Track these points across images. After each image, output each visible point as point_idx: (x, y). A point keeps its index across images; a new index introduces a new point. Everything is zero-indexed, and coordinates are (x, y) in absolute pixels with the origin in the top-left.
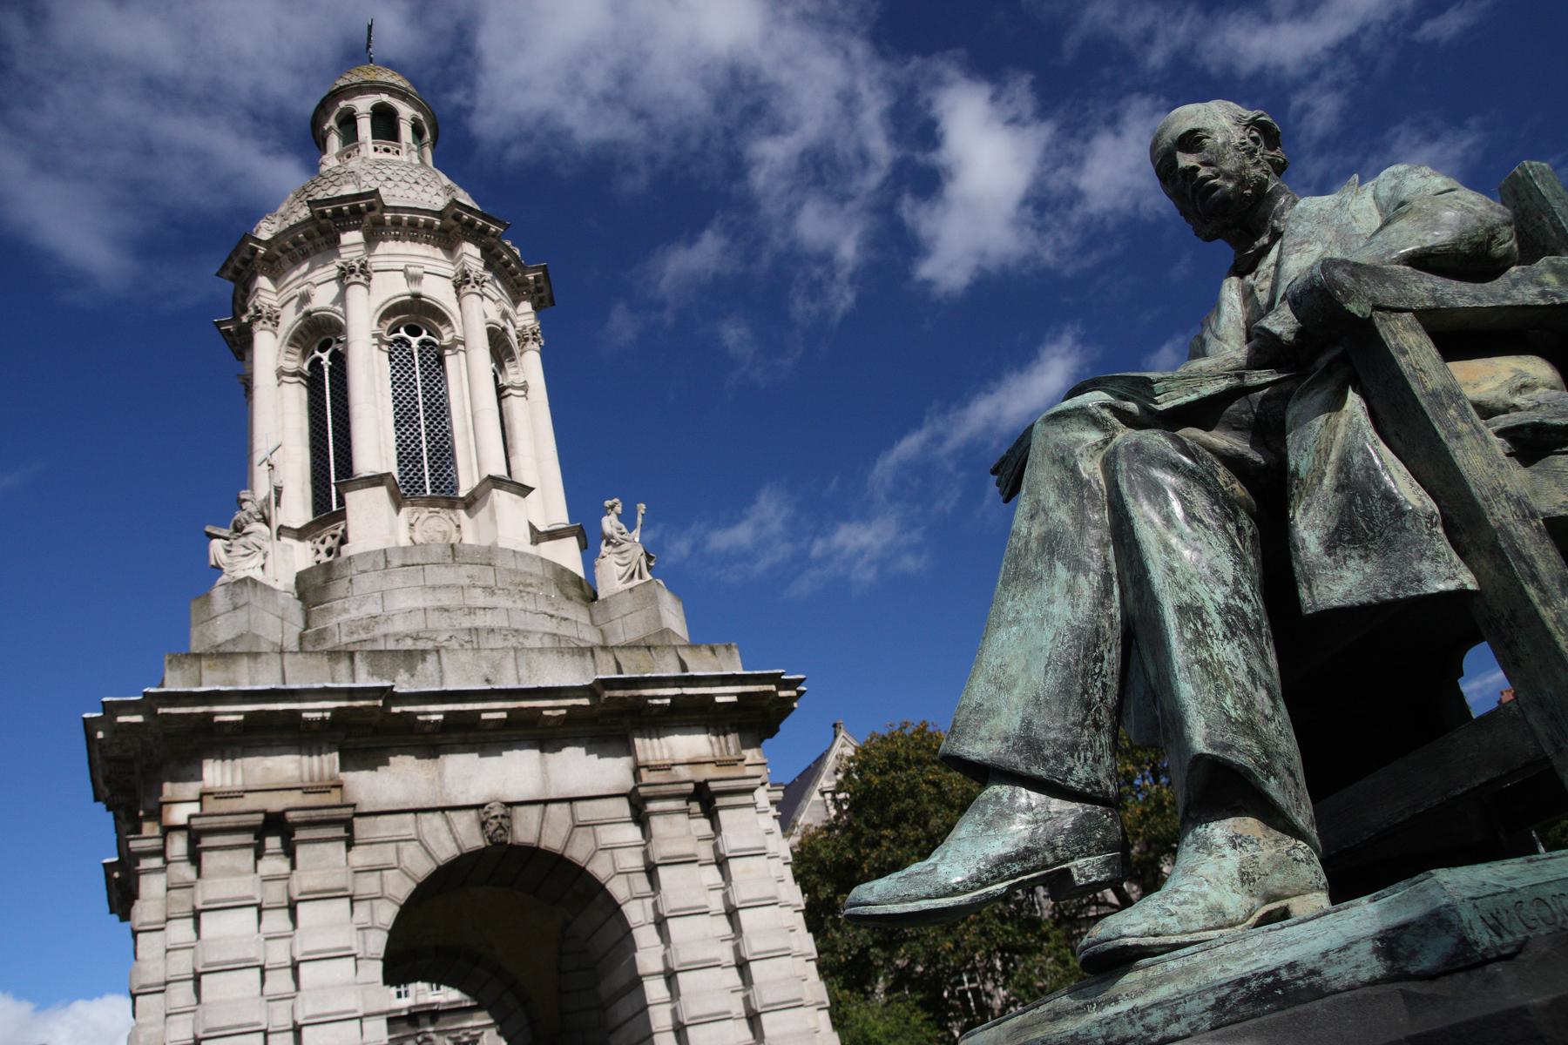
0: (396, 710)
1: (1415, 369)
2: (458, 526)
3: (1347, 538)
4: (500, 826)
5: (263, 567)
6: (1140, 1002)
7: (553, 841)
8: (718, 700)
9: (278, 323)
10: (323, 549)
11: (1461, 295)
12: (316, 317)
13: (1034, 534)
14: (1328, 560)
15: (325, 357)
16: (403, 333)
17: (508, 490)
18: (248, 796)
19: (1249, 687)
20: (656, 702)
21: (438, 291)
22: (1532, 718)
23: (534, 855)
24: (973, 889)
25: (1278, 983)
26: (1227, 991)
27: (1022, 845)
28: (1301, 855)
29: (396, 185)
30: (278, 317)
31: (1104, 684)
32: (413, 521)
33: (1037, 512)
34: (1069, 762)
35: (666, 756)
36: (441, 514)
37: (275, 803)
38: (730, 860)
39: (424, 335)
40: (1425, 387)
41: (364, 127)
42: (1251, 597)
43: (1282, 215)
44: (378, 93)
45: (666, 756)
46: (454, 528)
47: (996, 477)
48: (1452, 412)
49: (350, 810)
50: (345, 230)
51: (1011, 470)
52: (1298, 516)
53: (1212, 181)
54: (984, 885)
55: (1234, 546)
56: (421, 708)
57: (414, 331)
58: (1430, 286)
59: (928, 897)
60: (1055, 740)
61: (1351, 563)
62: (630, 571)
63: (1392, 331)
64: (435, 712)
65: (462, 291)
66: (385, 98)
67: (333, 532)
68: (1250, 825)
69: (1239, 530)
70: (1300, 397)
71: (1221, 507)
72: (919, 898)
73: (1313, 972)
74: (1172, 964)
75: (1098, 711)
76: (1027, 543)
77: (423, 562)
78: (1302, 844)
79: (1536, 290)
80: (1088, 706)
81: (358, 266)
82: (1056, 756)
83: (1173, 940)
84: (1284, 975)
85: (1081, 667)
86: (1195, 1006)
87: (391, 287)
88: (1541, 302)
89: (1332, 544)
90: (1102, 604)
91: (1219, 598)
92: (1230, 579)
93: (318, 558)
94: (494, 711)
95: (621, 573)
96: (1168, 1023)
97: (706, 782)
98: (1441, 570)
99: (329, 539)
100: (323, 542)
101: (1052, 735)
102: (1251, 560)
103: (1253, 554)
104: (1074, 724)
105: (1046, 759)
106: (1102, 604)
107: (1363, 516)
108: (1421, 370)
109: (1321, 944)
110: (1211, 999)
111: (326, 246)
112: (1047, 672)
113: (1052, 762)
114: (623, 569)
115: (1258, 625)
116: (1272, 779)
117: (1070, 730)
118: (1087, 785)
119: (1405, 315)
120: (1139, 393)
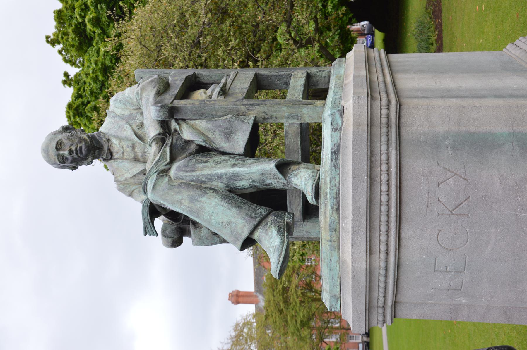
3: (228, 136)
6: (329, 186)
13: (187, 204)
14: (232, 143)
24: (284, 238)
25: (335, 153)
26: (333, 164)
33: (181, 202)
34: (258, 212)
47: (148, 235)
48: (207, 103)
51: (150, 227)
52: (215, 146)
53: (78, 147)
59: (282, 248)
60: (251, 213)
61: (235, 138)
69: (214, 155)
70: (182, 133)
72: (282, 250)
73: (335, 145)
74: (322, 180)
76: (189, 207)
79: (179, 81)
82: (256, 214)
83: (317, 178)
84: (333, 151)
86: (333, 172)
88: (183, 81)
92: (229, 158)
96: (335, 180)
105: (255, 217)
106: (218, 192)
107: (225, 129)
109: (329, 142)
110: (333, 168)
112: (231, 210)
113: (257, 215)
117: (250, 209)
118: (266, 211)
120: (160, 165)
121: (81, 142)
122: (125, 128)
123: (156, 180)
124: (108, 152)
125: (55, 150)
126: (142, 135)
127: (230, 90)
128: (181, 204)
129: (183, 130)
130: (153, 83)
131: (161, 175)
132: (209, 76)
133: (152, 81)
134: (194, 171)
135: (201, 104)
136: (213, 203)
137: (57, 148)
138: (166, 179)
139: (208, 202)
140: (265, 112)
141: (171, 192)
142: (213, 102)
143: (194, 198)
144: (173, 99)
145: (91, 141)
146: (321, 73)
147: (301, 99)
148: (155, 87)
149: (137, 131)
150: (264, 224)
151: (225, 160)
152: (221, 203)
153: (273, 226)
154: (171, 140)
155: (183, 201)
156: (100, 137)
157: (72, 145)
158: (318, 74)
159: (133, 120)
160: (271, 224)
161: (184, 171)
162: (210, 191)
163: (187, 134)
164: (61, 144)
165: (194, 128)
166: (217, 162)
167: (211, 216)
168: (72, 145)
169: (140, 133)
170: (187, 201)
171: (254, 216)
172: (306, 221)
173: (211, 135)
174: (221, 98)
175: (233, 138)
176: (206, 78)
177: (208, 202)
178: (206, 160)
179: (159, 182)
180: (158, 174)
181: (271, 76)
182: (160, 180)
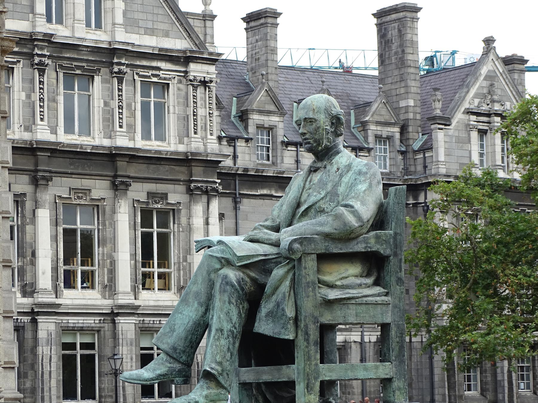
1: (306, 274)
13: (193, 290)
14: (264, 319)
19: (227, 352)
22: (296, 371)
24: (151, 381)
27: (165, 372)
28: (223, 393)
31: (197, 337)
40: (306, 280)
42: (237, 328)
43: (331, 157)
48: (310, 289)
52: (263, 303)
53: (309, 140)
54: (153, 380)
55: (240, 312)
58: (326, 244)
59: (140, 380)
63: (305, 261)
68: (213, 385)
69: (243, 307)
71: (240, 301)
72: (138, 380)
75: (193, 344)
76: (190, 291)
78: (224, 390)
79: (364, 245)
80: (191, 342)
82: (179, 353)
85: (192, 332)
88: (363, 250)
89: (267, 315)
90: (203, 317)
91: (229, 327)
92: (234, 323)
98: (286, 333)
101: (180, 348)
102: (243, 316)
103: (245, 314)
104: (186, 346)
105: (177, 353)
107: (276, 311)
108: (308, 275)
112: (183, 331)
113: (178, 354)
115: (236, 335)
116: (221, 376)
117: (184, 347)
118: (185, 361)
119: (313, 255)
121: (315, 141)
122: (322, 192)
123: (217, 257)
124: (316, 167)
125: (304, 118)
126: (310, 214)
127: (341, 306)
128: (195, 284)
129: (280, 269)
130: (342, 227)
131: (223, 261)
132: (389, 271)
133: (345, 224)
134: (220, 292)
135: (308, 283)
136: (191, 314)
137: (306, 119)
138: (218, 266)
139: (193, 309)
140: (300, 347)
141: (205, 273)
142: (311, 294)
143: (198, 296)
144: (319, 252)
145: (322, 150)
146: (392, 393)
147: (321, 379)
148: (336, 229)
149: (314, 207)
150: (172, 360)
151: (231, 319)
152: (191, 321)
153: (167, 369)
154: (274, 257)
155: (196, 285)
156: (331, 156)
157: (311, 133)
158: (392, 390)
159: (330, 199)
160: (169, 367)
161: (221, 283)
162: (203, 309)
163: (278, 272)
164: (311, 122)
165: (281, 281)
166: (229, 312)
167: (181, 313)
168: (311, 133)
169: (312, 210)
170: (196, 289)
171: (178, 351)
172: (240, 386)
173: (274, 297)
175: (268, 320)
176: (387, 268)
177: (193, 309)
178: (233, 301)
179: (215, 260)
180: (223, 258)
181: (389, 339)
182: (217, 261)
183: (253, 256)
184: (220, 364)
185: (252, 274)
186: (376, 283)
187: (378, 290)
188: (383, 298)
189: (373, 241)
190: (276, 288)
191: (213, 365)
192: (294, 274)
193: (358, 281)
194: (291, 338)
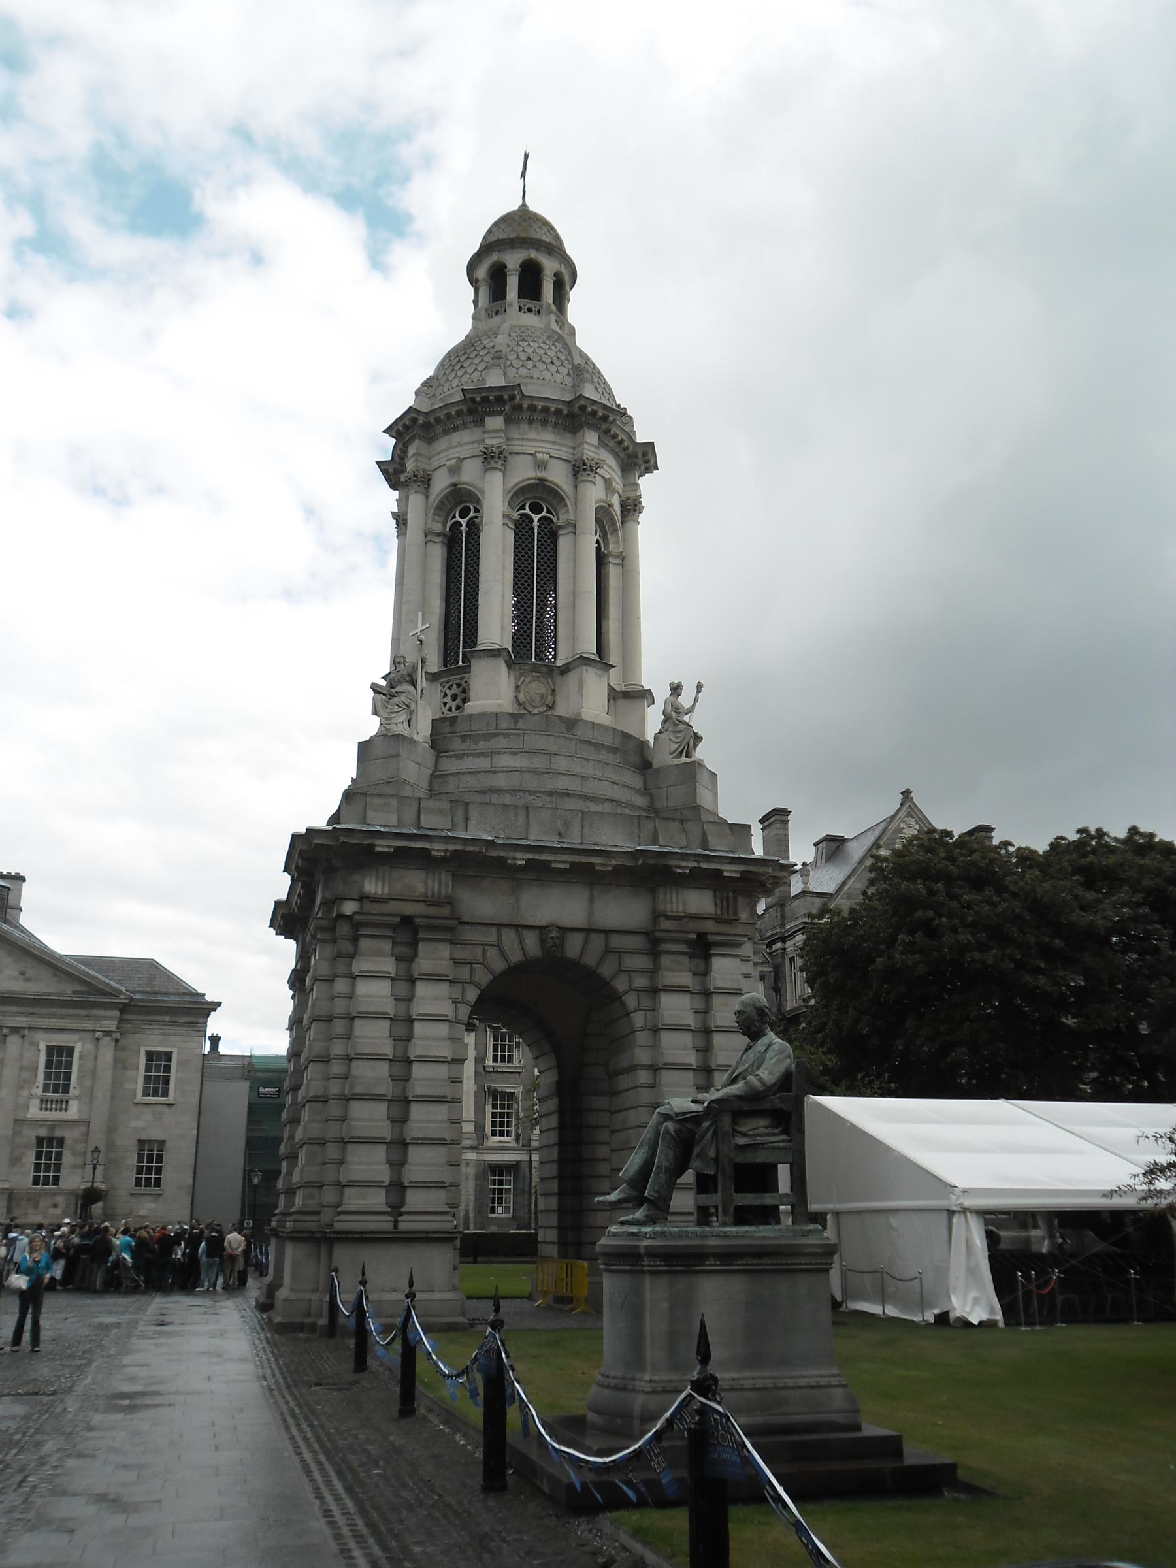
0: (493, 854)
2: (554, 690)
4: (555, 945)
5: (409, 721)
7: (590, 960)
8: (726, 874)
9: (429, 485)
10: (450, 694)
11: (746, 1107)
12: (460, 489)
15: (464, 522)
16: (528, 511)
17: (594, 667)
18: (391, 902)
20: (679, 870)
21: (558, 475)
23: (574, 965)
29: (535, 366)
30: (429, 480)
32: (519, 683)
35: (681, 909)
36: (542, 679)
37: (409, 909)
38: (713, 995)
39: (544, 513)
41: (513, 283)
44: (528, 249)
45: (681, 909)
46: (550, 691)
49: (456, 922)
50: (490, 414)
56: (511, 854)
57: (536, 509)
62: (680, 749)
64: (521, 858)
65: (580, 478)
66: (533, 254)
67: (458, 681)
77: (524, 728)
81: (497, 452)
87: (523, 472)
93: (445, 700)
94: (561, 862)
95: (673, 749)
97: (707, 934)
99: (455, 686)
100: (450, 688)
111: (473, 424)
114: (675, 746)
174: (733, 1146)
183: (684, 1113)
184: (658, 1192)
185: (689, 1126)
186: (783, 1133)
187: (783, 1137)
188: (786, 1144)
189: (777, 1101)
190: (703, 1137)
191: (652, 1193)
192: (717, 1127)
193: (771, 1131)
194: (712, 1173)
